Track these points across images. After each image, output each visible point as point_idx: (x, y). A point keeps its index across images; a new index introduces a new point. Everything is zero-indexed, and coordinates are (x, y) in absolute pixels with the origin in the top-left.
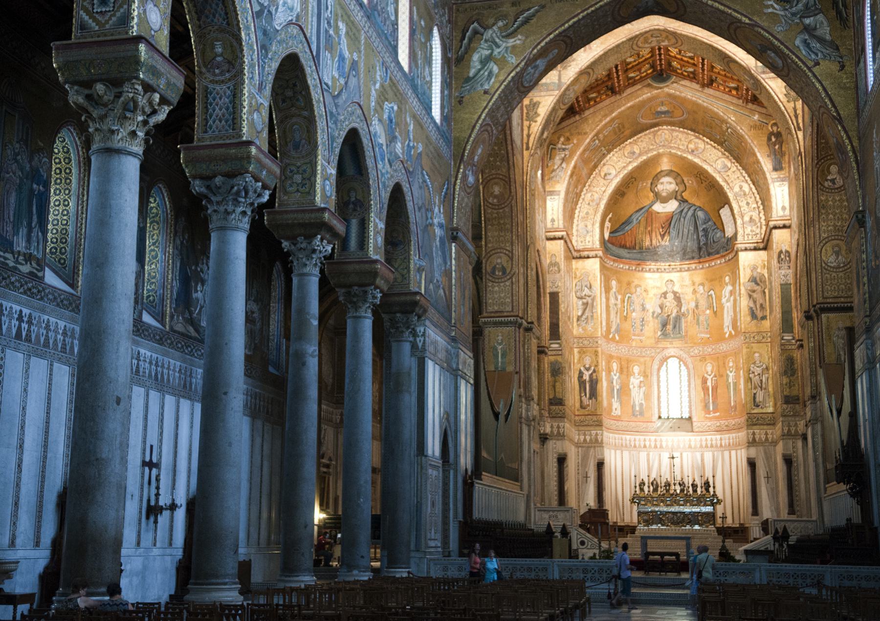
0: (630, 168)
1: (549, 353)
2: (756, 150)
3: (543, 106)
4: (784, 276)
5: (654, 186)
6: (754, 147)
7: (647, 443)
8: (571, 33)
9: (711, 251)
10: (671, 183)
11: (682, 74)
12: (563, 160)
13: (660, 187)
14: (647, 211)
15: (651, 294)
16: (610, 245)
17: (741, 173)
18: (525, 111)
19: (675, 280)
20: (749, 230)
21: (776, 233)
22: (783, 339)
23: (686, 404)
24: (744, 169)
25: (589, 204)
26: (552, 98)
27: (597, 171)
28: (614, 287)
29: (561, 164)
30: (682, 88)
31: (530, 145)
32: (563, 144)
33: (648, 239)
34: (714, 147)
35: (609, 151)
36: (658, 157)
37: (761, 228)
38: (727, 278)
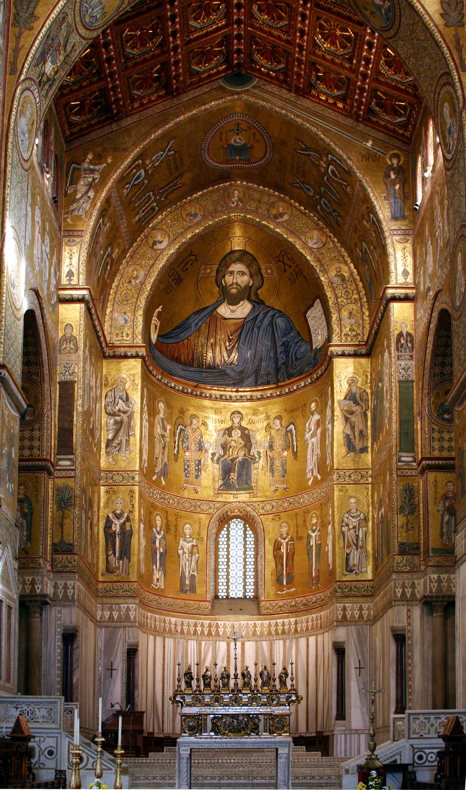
1: (56, 474)
4: (403, 369)
5: (221, 276)
6: (366, 186)
9: (293, 372)
10: (243, 274)
11: (268, 75)
13: (229, 279)
15: (211, 426)
19: (243, 413)
20: (348, 329)
21: (396, 307)
22: (400, 461)
27: (142, 235)
28: (162, 411)
30: (267, 96)
32: (91, 163)
35: (162, 208)
38: (313, 405)
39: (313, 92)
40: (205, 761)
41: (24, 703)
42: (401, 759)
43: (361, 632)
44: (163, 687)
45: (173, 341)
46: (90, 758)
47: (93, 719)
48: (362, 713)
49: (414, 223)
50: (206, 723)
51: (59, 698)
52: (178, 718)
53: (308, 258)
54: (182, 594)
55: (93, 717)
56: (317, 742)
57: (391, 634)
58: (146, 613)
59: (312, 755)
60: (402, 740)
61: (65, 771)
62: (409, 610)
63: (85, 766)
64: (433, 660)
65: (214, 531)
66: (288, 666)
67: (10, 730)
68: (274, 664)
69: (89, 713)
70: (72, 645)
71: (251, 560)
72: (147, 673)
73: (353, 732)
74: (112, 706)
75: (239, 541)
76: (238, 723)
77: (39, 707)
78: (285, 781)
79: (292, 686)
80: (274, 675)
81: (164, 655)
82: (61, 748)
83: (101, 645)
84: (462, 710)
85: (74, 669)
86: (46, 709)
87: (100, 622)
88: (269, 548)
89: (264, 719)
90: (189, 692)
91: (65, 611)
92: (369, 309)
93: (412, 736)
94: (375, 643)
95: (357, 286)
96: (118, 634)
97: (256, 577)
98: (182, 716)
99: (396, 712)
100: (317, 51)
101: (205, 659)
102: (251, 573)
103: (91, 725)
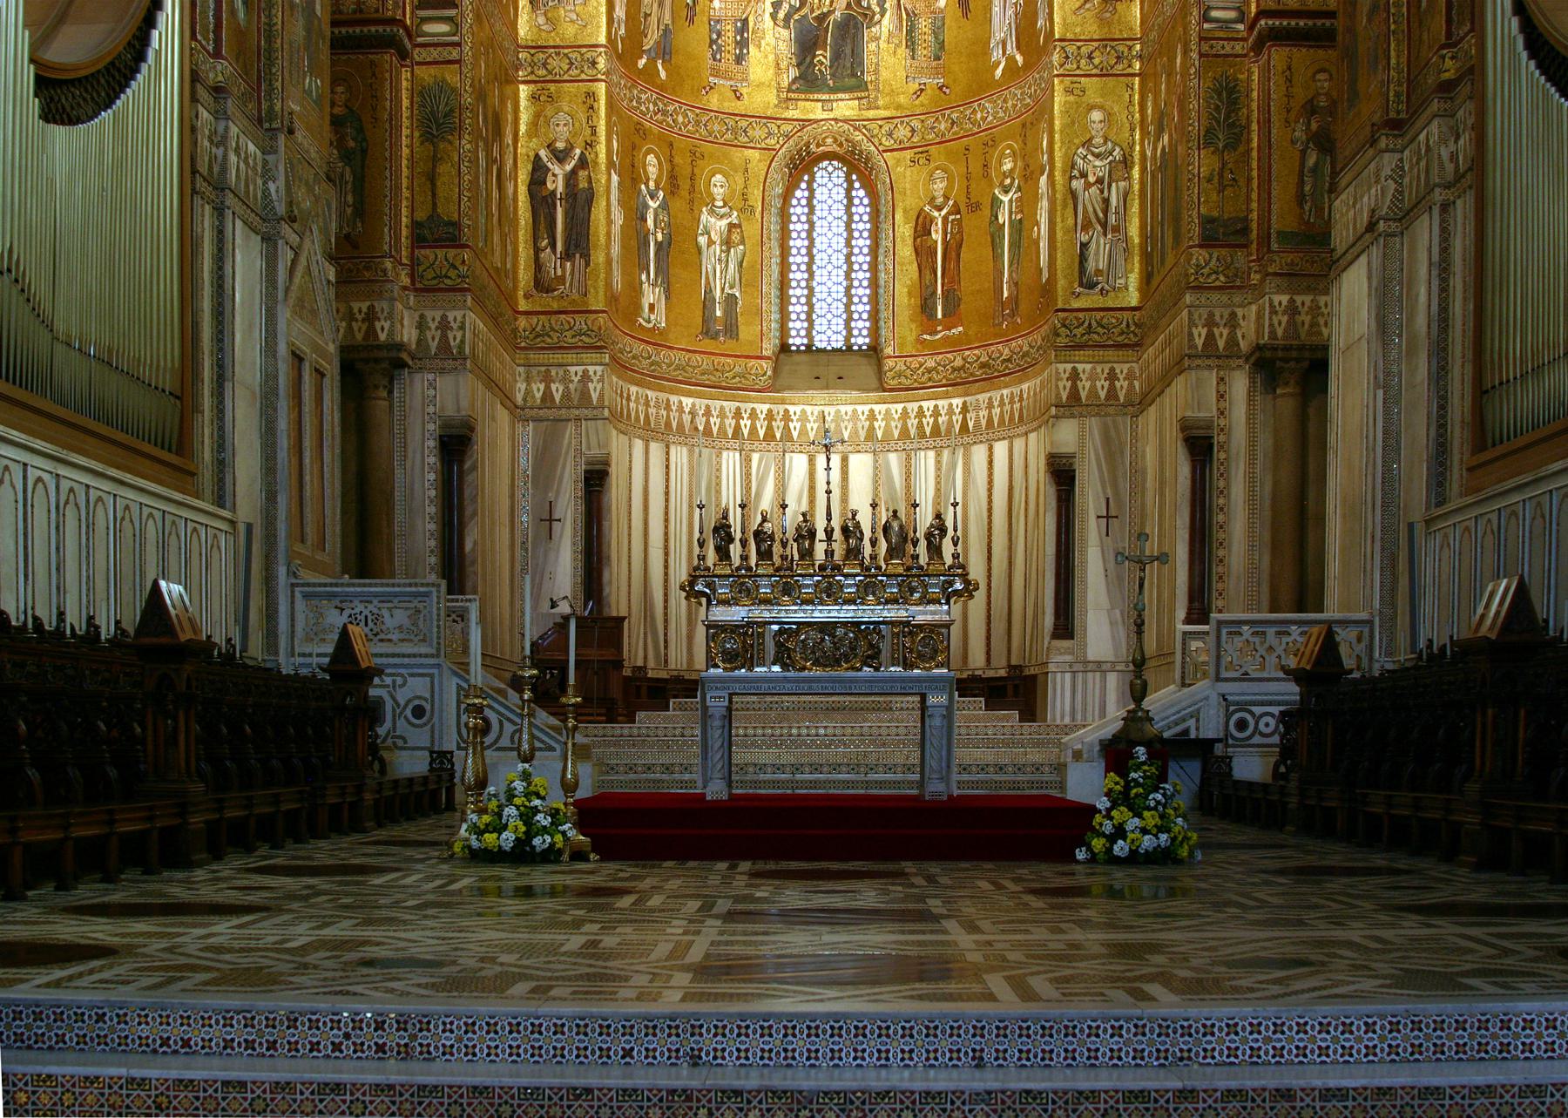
7: (745, 423)
23: (862, 308)
40: (760, 732)
41: (356, 595)
42: (1197, 729)
43: (1113, 433)
44: (666, 561)
46: (506, 724)
47: (512, 636)
48: (1111, 623)
50: (763, 643)
51: (433, 585)
52: (701, 632)
54: (707, 341)
55: (511, 629)
56: (1010, 691)
57: (1180, 435)
58: (626, 386)
59: (1000, 719)
60: (1200, 684)
61: (452, 752)
62: (1222, 379)
63: (496, 741)
64: (1274, 499)
65: (779, 190)
66: (946, 513)
67: (327, 660)
68: (915, 506)
69: (501, 623)
70: (461, 463)
71: (862, 260)
72: (630, 528)
73: (1090, 667)
74: (554, 605)
75: (835, 214)
76: (834, 643)
77: (390, 605)
78: (941, 772)
79: (955, 556)
80: (915, 532)
81: (667, 487)
82: (441, 700)
83: (525, 462)
84: (1337, 616)
85: (466, 519)
86: (407, 609)
87: (523, 409)
88: (905, 230)
89: (893, 634)
90: (723, 572)
91: (444, 383)
93: (1224, 675)
94: (1144, 456)
96: (563, 437)
97: (874, 299)
98: (708, 627)
99: (1188, 621)
101: (759, 495)
102: (862, 292)
103: (507, 649)
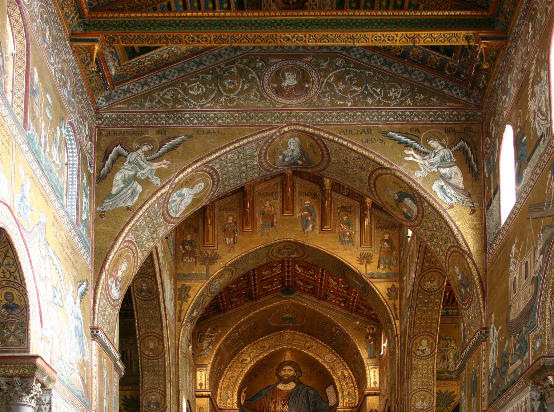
0: (262, 357)
2: (357, 345)
3: (194, 290)
6: (356, 343)
8: (218, 166)
10: (291, 370)
12: (210, 343)
14: (273, 388)
16: (245, 409)
17: (343, 364)
18: (178, 293)
24: (345, 361)
25: (230, 379)
26: (201, 285)
29: (208, 346)
31: (182, 319)
32: (210, 332)
33: (273, 407)
34: (324, 346)
36: (283, 350)
37: (355, 399)
39: (328, 299)
45: (253, 402)
49: (380, 361)
53: (326, 367)
92: (358, 391)
95: (352, 380)
100: (330, 285)
